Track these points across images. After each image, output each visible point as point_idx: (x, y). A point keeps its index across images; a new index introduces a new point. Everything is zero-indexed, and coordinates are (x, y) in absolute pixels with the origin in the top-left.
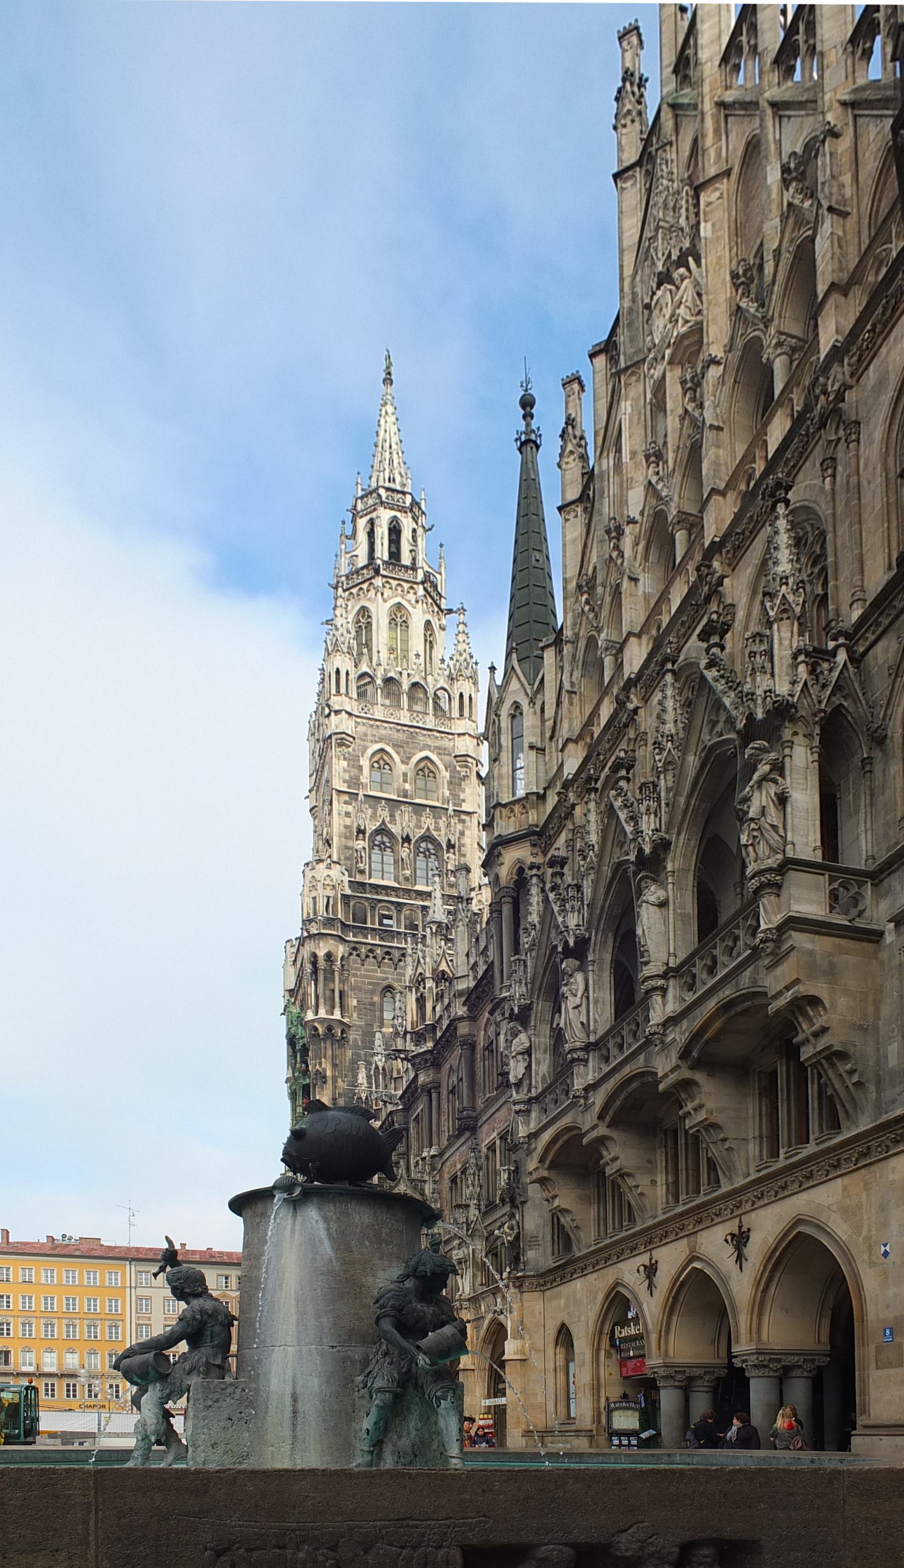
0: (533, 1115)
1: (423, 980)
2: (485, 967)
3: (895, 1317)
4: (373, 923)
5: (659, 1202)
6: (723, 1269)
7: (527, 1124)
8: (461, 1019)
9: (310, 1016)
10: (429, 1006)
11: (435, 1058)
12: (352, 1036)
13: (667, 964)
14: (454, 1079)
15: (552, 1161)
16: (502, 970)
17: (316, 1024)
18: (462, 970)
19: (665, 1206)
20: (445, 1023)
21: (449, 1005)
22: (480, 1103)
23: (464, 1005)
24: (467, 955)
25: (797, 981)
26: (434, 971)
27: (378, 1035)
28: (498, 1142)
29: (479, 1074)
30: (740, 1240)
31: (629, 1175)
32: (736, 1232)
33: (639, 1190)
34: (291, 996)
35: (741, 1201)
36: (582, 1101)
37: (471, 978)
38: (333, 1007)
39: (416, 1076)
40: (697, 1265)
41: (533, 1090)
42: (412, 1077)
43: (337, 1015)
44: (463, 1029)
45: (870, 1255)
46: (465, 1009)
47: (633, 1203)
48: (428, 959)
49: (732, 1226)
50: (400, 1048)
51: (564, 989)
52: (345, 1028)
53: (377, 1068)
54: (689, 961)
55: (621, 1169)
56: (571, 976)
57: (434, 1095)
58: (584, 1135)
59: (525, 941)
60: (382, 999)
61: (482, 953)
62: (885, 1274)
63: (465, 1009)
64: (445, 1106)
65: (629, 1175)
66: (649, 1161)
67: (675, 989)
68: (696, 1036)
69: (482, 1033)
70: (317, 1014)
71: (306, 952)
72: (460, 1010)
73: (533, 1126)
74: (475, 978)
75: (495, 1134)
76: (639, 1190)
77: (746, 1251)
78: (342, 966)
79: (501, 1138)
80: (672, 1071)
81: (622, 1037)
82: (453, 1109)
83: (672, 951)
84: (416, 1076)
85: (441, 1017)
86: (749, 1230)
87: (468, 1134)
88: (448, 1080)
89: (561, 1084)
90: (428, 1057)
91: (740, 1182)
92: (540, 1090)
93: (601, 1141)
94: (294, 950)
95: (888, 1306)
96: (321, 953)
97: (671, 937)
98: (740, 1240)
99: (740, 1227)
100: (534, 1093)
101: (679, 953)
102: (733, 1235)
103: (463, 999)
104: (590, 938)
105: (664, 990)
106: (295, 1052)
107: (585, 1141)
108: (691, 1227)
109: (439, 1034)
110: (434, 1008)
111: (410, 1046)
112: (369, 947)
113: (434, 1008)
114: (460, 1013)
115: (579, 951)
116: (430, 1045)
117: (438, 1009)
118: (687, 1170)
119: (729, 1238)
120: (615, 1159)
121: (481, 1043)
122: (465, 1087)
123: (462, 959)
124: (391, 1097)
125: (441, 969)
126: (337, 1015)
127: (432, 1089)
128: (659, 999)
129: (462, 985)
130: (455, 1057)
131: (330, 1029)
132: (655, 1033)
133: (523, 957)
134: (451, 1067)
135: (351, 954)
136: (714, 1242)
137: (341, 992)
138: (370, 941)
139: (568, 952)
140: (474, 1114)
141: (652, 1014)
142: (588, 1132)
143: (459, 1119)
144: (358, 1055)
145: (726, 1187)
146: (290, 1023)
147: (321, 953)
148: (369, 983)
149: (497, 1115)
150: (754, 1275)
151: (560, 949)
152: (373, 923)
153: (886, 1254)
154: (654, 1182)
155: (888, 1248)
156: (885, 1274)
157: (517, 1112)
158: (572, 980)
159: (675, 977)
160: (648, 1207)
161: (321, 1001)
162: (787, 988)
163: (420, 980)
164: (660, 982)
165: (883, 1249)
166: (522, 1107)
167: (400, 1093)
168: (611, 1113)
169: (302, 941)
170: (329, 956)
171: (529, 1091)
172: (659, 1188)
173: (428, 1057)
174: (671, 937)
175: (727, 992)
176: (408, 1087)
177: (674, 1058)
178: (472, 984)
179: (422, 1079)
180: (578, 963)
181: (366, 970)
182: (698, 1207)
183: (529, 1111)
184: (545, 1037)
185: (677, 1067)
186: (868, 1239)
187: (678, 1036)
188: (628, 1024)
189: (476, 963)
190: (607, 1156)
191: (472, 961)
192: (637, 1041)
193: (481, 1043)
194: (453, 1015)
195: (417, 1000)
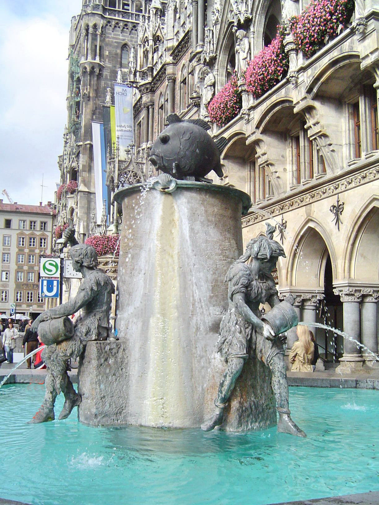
1: (148, 41)
4: (119, 8)
5: (288, 182)
6: (328, 229)
9: (83, 60)
10: (150, 56)
11: (152, 87)
12: (106, 73)
14: (162, 100)
16: (197, 36)
17: (86, 65)
18: (170, 36)
19: (291, 185)
20: (159, 66)
21: (162, 55)
23: (171, 55)
26: (154, 36)
27: (119, 72)
30: (338, 210)
31: (272, 165)
32: (336, 204)
33: (277, 175)
34: (73, 49)
35: (338, 185)
36: (247, 117)
37: (175, 40)
38: (95, 55)
39: (141, 98)
40: (311, 225)
43: (97, 60)
44: (170, 70)
46: (171, 58)
47: (272, 182)
49: (333, 201)
50: (132, 80)
51: (237, 47)
52: (101, 68)
55: (267, 161)
56: (241, 40)
57: (151, 110)
58: (246, 139)
59: (212, 18)
60: (121, 52)
63: (171, 58)
65: (272, 165)
66: (283, 156)
69: (180, 72)
70: (87, 60)
71: (83, 23)
72: (169, 59)
76: (277, 175)
77: (341, 217)
78: (102, 31)
80: (302, 100)
82: (161, 118)
84: (141, 98)
85: (157, 62)
86: (343, 204)
88: (159, 101)
90: (148, 86)
91: (339, 172)
93: (257, 142)
94: (77, 22)
96: (91, 25)
98: (338, 210)
99: (338, 201)
102: (334, 207)
104: (252, 18)
106: (73, 82)
107: (247, 142)
108: (308, 200)
109: (155, 73)
110: (153, 57)
111: (138, 79)
112: (117, 21)
113: (153, 57)
115: (246, 25)
116: (150, 79)
118: (305, 163)
119: (332, 208)
120: (264, 154)
121: (179, 79)
125: (157, 35)
126: (97, 60)
127: (150, 106)
130: (164, 87)
131: (93, 68)
132: (292, 77)
133: (212, 28)
134: (161, 93)
135: (107, 25)
136: (321, 211)
137: (100, 47)
139: (240, 26)
141: (291, 65)
142: (249, 136)
144: (107, 84)
145: (330, 175)
146: (72, 64)
147: (91, 25)
148: (116, 42)
150: (346, 234)
151: (235, 24)
152: (119, 8)
154: (285, 170)
158: (242, 43)
160: (282, 187)
161: (89, 52)
163: (146, 41)
168: (263, 124)
169: (81, 17)
170: (95, 26)
172: (288, 174)
173: (148, 86)
177: (303, 93)
178: (176, 44)
180: (245, 33)
181: (114, 35)
182: (312, 188)
184: (222, 75)
190: (259, 151)
193: (179, 79)
195: (144, 52)
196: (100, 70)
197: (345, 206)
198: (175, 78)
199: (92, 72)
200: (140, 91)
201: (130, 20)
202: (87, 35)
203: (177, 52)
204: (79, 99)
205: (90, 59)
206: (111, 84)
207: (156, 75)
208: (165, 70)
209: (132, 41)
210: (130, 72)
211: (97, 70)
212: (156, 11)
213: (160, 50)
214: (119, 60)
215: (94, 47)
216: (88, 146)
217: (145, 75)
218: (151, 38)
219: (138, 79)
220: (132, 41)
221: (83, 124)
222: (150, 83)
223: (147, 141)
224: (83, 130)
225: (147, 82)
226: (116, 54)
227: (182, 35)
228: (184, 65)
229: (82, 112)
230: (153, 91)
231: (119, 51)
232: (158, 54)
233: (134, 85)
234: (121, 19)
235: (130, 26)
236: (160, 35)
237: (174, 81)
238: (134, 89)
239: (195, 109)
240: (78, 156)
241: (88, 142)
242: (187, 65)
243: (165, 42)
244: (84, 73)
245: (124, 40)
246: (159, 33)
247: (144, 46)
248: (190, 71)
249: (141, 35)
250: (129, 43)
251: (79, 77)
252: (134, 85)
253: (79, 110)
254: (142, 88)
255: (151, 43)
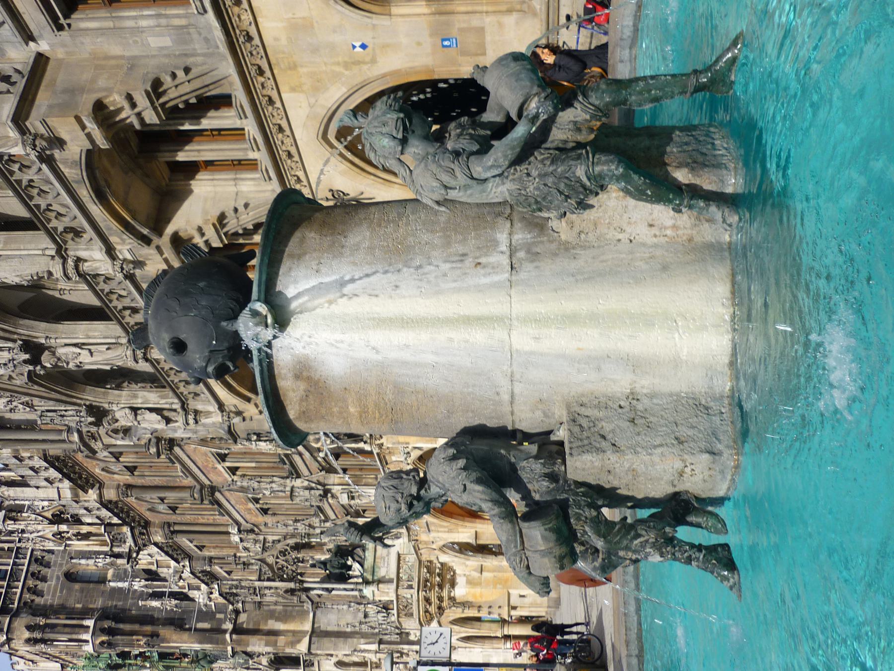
0: (200, 407)
1: (60, 533)
2: (52, 470)
3: (431, 35)
7: (208, 414)
8: (100, 496)
10: (85, 529)
11: (140, 525)
13: (53, 257)
15: (249, 391)
18: (52, 493)
20: (105, 513)
21: (86, 509)
22: (188, 481)
23: (86, 492)
24: (37, 488)
25: (78, 119)
26: (51, 522)
27: (112, 584)
28: (228, 464)
29: (157, 481)
37: (60, 485)
38: (82, 626)
41: (174, 407)
42: (156, 549)
43: (90, 623)
44: (110, 494)
45: (364, 63)
46: (90, 491)
48: (40, 527)
50: (125, 561)
53: (146, 586)
54: (51, 234)
57: (177, 528)
61: (36, 472)
62: (385, 46)
63: (90, 491)
64: (188, 518)
67: (78, 250)
68: (127, 227)
72: (92, 495)
73: (213, 407)
74: (61, 480)
75: (219, 467)
79: (224, 461)
81: (125, 308)
82: (191, 509)
83: (40, 252)
85: (98, 518)
87: (218, 495)
89: (168, 376)
90: (137, 532)
92: (176, 401)
95: (419, 44)
97: (25, 252)
100: (177, 406)
101: (44, 246)
103: (81, 492)
105: (78, 260)
109: (115, 520)
110: (89, 524)
112: (25, 590)
113: (89, 524)
114: (95, 497)
116: (126, 530)
117: (89, 520)
122: (171, 496)
123: (41, 493)
124: (176, 572)
125: (50, 517)
126: (90, 623)
127: (171, 530)
128: (86, 264)
129: (67, 493)
131: (103, 631)
134: (149, 510)
138: (19, 591)
140: (198, 487)
143: (202, 500)
148: (61, 592)
149: (200, 465)
153: (364, 46)
155: (358, 44)
156: (385, 46)
157: (197, 422)
159: (66, 249)
162: (83, 127)
164: (70, 263)
165: (358, 49)
166: (191, 418)
167: (173, 563)
171: (175, 410)
174: (25, 252)
175: (85, 193)
176: (167, 553)
178: (67, 484)
179: (159, 538)
183: (196, 412)
184: (120, 396)
185: (158, 248)
186: (346, 65)
187: (125, 247)
188: (111, 301)
189: (47, 480)
191: (45, 483)
192: (130, 293)
194: (99, 505)
195: (78, 540)
196: (108, 618)
197: (334, 189)
198: (125, 485)
199: (110, 632)
200: (145, 545)
201: (25, 568)
202: (43, 641)
203: (82, 481)
204: (155, 655)
205: (87, 636)
206: (132, 599)
207: (120, 518)
208: (110, 502)
209: (61, 565)
210: (112, 564)
211: (106, 624)
212: (11, 519)
213: (76, 512)
214: (92, 585)
215: (67, 630)
216: (234, 636)
217: (119, 537)
218: (55, 528)
219: (124, 549)
220: (61, 565)
221: (197, 646)
222: (132, 530)
223: (228, 533)
224: (208, 647)
225: (129, 534)
226: (82, 590)
227: (53, 473)
228: (103, 470)
229: (177, 648)
230: (147, 524)
231: (77, 586)
232: (83, 515)
233: (134, 555)
234: (21, 584)
235: (35, 568)
236: (51, 512)
237: (129, 486)
238: (140, 557)
239: (177, 449)
240: (250, 655)
241: (228, 636)
242: (102, 465)
243: (63, 502)
244: (110, 645)
245: (58, 578)
246: (48, 515)
247: (69, 539)
248: (114, 460)
249: (50, 546)
250: (65, 568)
251: (118, 655)
252: (134, 555)
253: (173, 654)
254: (140, 542)
255: (63, 528)
